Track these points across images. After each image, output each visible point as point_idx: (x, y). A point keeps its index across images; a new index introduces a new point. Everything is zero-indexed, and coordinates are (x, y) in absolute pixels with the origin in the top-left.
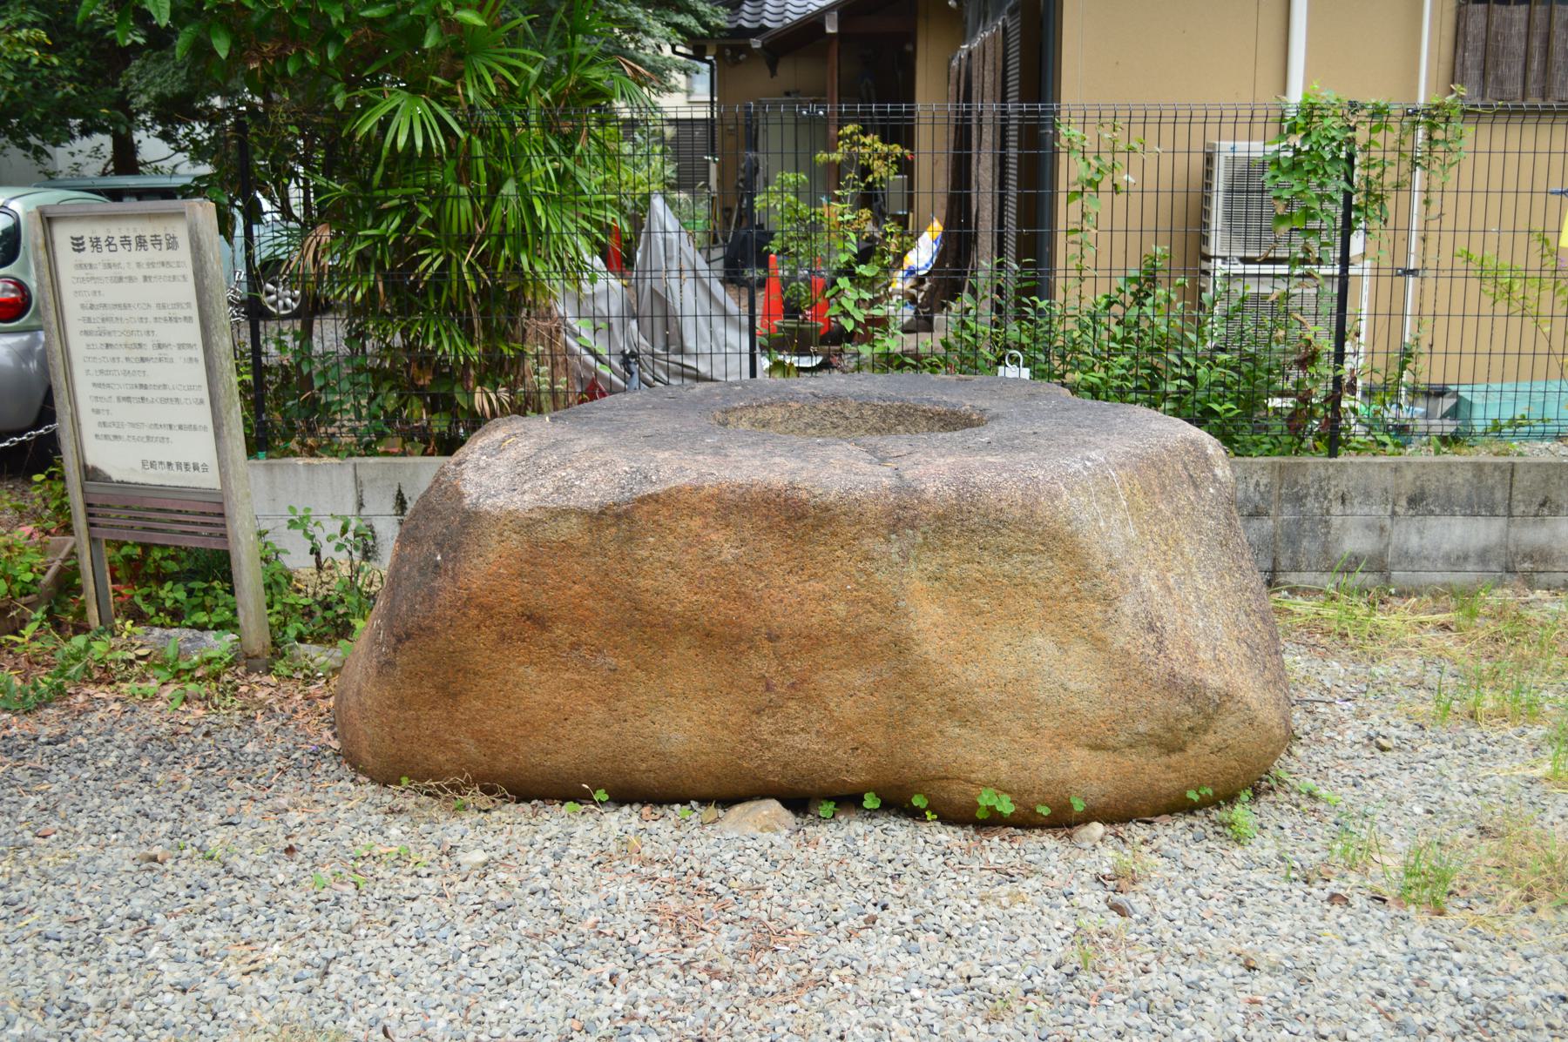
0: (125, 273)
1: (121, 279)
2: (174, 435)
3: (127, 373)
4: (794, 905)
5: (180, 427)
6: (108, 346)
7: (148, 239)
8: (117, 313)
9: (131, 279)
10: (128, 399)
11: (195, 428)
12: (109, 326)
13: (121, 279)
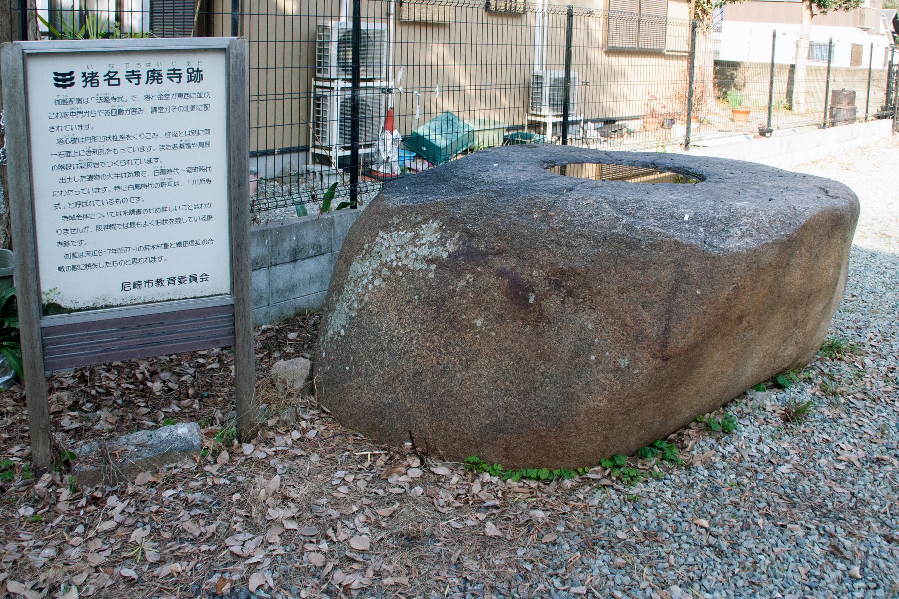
0: (125, 106)
1: (121, 111)
2: (174, 251)
3: (112, 201)
4: (726, 566)
5: (179, 244)
6: (91, 177)
7: (164, 73)
8: (111, 144)
9: (134, 111)
10: (113, 226)
11: (197, 242)
12: (95, 158)
13: (121, 111)
